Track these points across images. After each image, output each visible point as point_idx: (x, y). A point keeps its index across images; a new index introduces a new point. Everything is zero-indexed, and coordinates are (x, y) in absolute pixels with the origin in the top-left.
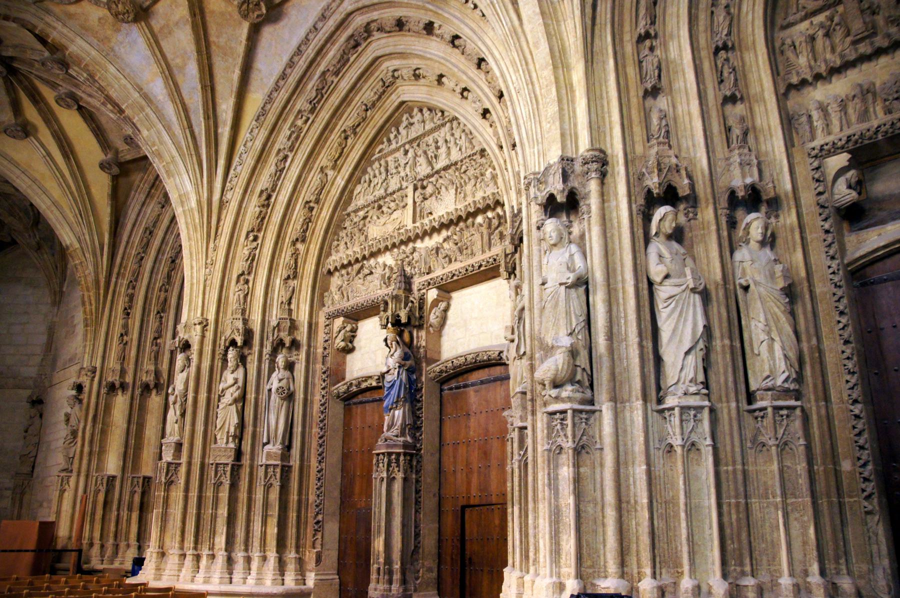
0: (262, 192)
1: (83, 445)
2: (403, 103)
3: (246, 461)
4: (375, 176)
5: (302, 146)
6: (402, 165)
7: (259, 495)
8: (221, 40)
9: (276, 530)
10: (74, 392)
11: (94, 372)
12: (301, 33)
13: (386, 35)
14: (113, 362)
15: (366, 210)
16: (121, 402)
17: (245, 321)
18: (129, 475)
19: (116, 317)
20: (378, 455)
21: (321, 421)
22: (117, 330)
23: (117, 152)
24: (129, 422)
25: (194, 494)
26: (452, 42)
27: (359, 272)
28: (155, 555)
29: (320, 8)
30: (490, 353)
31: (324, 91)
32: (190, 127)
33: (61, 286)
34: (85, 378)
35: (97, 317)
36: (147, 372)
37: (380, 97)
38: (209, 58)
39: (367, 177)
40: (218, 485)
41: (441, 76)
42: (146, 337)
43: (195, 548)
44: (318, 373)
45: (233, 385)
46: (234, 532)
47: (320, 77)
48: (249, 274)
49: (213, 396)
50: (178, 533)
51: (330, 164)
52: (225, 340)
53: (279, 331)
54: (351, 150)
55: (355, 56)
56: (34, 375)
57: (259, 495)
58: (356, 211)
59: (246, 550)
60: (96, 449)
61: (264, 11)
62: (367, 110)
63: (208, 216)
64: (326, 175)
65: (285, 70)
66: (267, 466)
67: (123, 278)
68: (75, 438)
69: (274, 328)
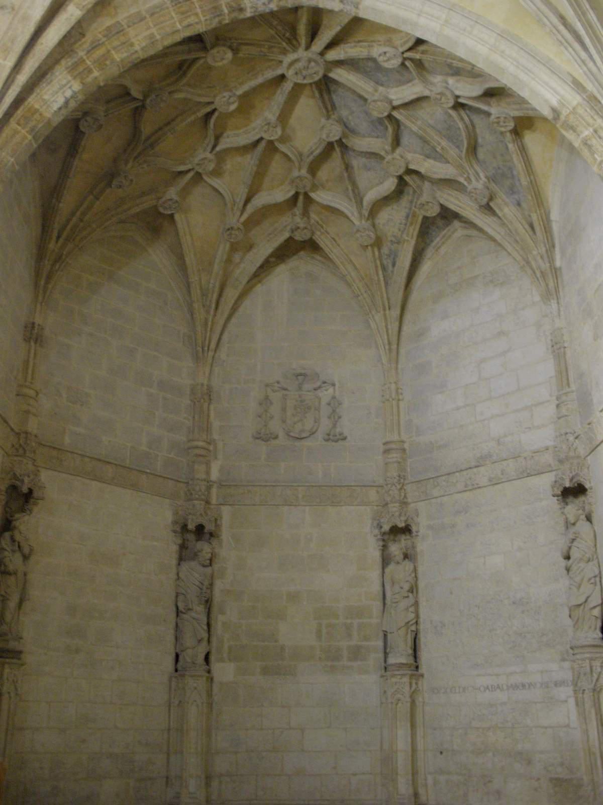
33: (551, 260)
56: (550, 443)
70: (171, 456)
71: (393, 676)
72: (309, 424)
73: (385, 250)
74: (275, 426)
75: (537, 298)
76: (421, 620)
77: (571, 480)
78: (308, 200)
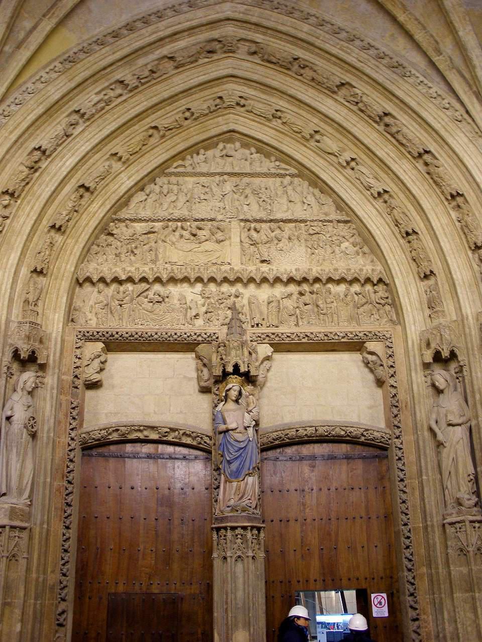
5: (100, 121)
20: (233, 528)
30: (352, 430)
31: (155, 75)
55: (207, 60)
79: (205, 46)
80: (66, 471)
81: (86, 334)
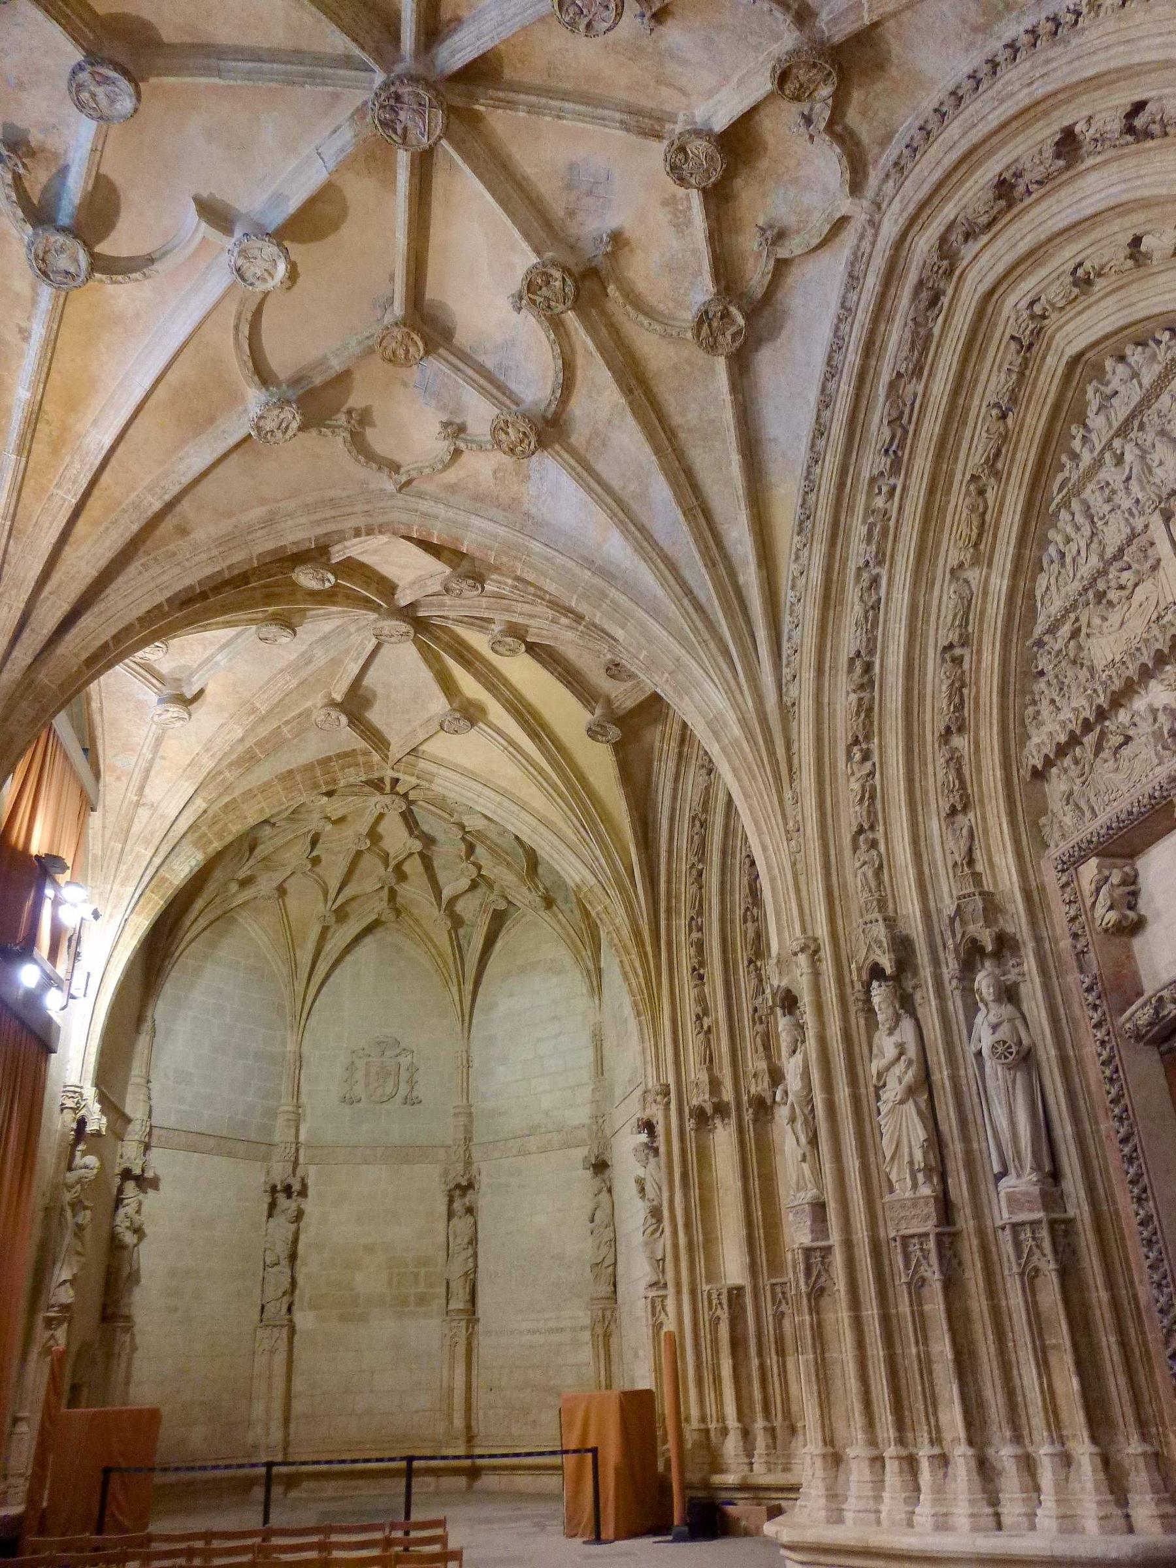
0: (851, 661)
1: (675, 1233)
2: (1077, 359)
3: (965, 1222)
4: (1068, 540)
6: (1118, 485)
7: (1015, 1298)
8: (690, 416)
9: (1075, 1384)
10: (644, 1137)
11: (667, 1094)
12: (824, 333)
13: (985, 239)
14: (696, 1072)
15: (1072, 616)
16: (723, 1138)
17: (891, 923)
18: (766, 1281)
19: (681, 989)
21: (1115, 1101)
22: (689, 1009)
23: (609, 702)
24: (745, 1177)
25: (871, 1312)
26: (1130, 129)
27: (1099, 748)
28: (819, 1462)
29: (842, 268)
31: (905, 420)
32: (689, 592)
34: (655, 1107)
35: (651, 996)
36: (755, 1075)
37: (1021, 374)
38: (680, 454)
39: (1052, 550)
40: (917, 1286)
41: (1137, 241)
42: (740, 1010)
43: (901, 1441)
44: (1077, 997)
45: (898, 1059)
46: (979, 1394)
47: (887, 397)
48: (872, 828)
49: (863, 1090)
50: (858, 1407)
51: (967, 556)
52: (859, 969)
53: (964, 923)
54: (1000, 512)
55: (941, 319)
56: (587, 1121)
57: (1015, 1298)
58: (1052, 630)
59: (1018, 1439)
60: (699, 1237)
61: (741, 321)
62: (1004, 417)
63: (765, 741)
64: (966, 581)
65: (818, 416)
66: (1016, 1227)
67: (678, 914)
68: (660, 1221)
69: (952, 920)
70: (265, 1120)
71: (453, 1320)
72: (389, 1089)
73: (461, 932)
74: (359, 1090)
75: (585, 991)
76: (479, 1270)
77: (597, 1157)
78: (393, 894)
79: (916, 309)
80: (1107, 1102)
81: (1064, 859)
